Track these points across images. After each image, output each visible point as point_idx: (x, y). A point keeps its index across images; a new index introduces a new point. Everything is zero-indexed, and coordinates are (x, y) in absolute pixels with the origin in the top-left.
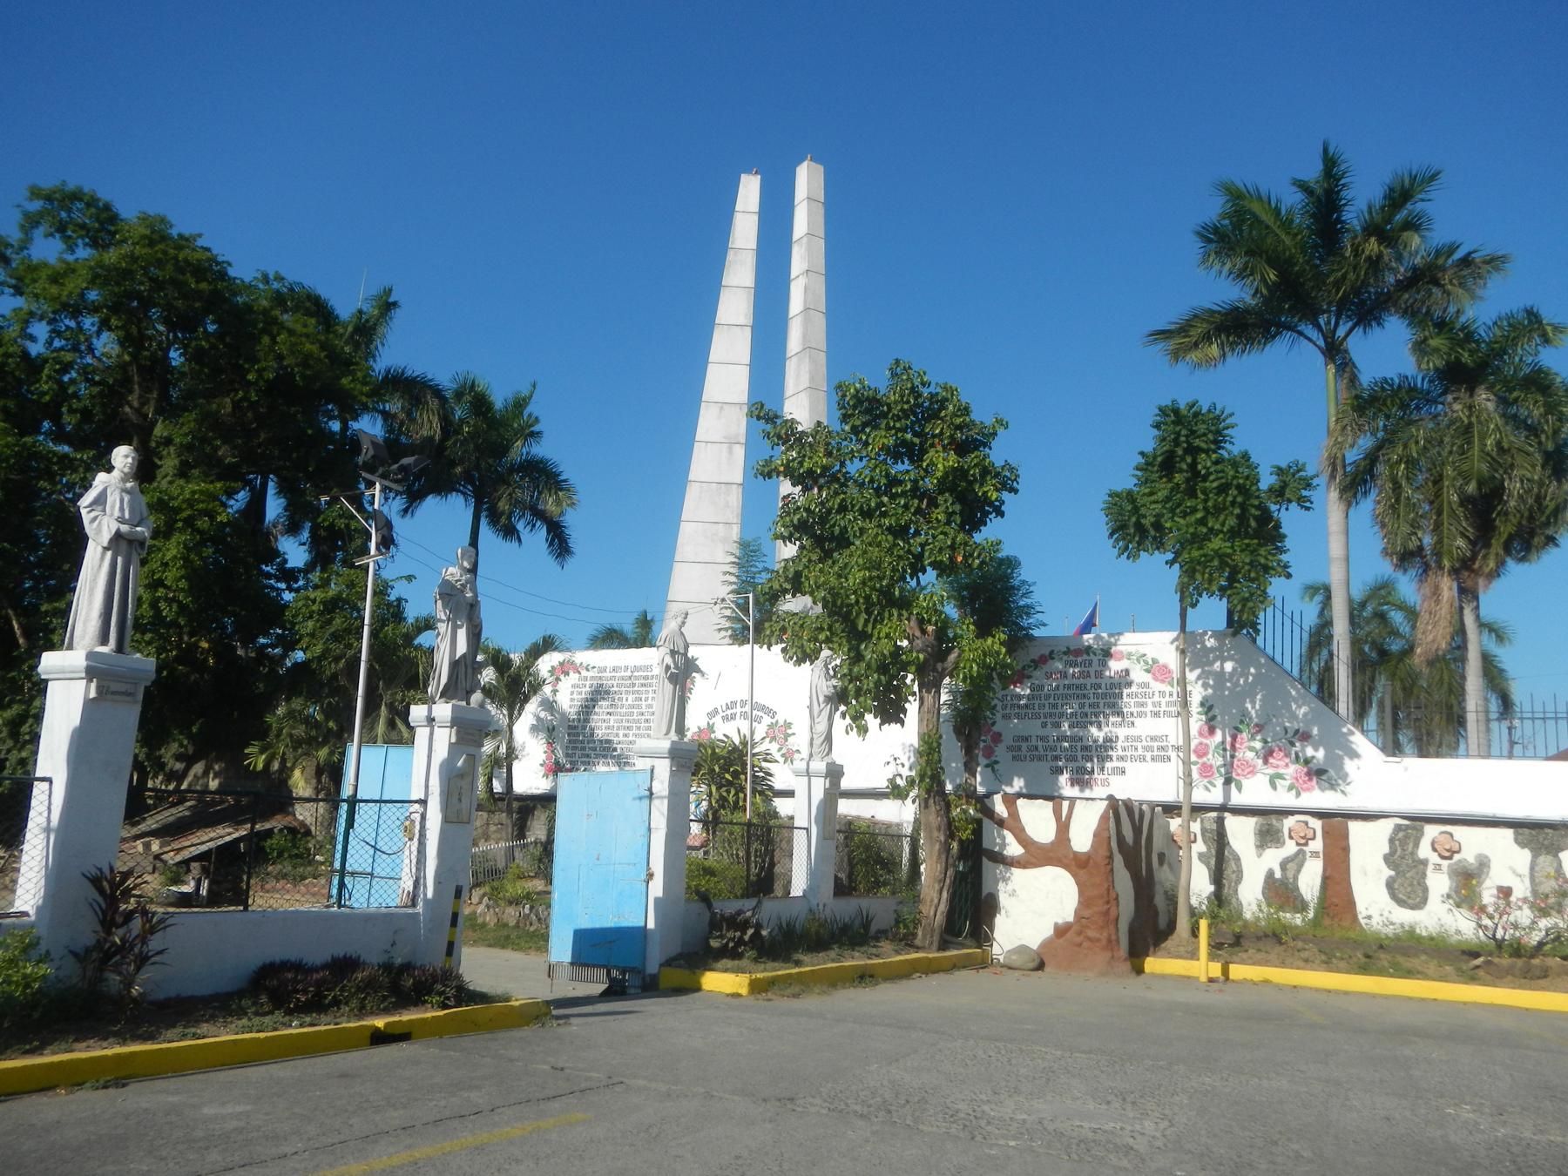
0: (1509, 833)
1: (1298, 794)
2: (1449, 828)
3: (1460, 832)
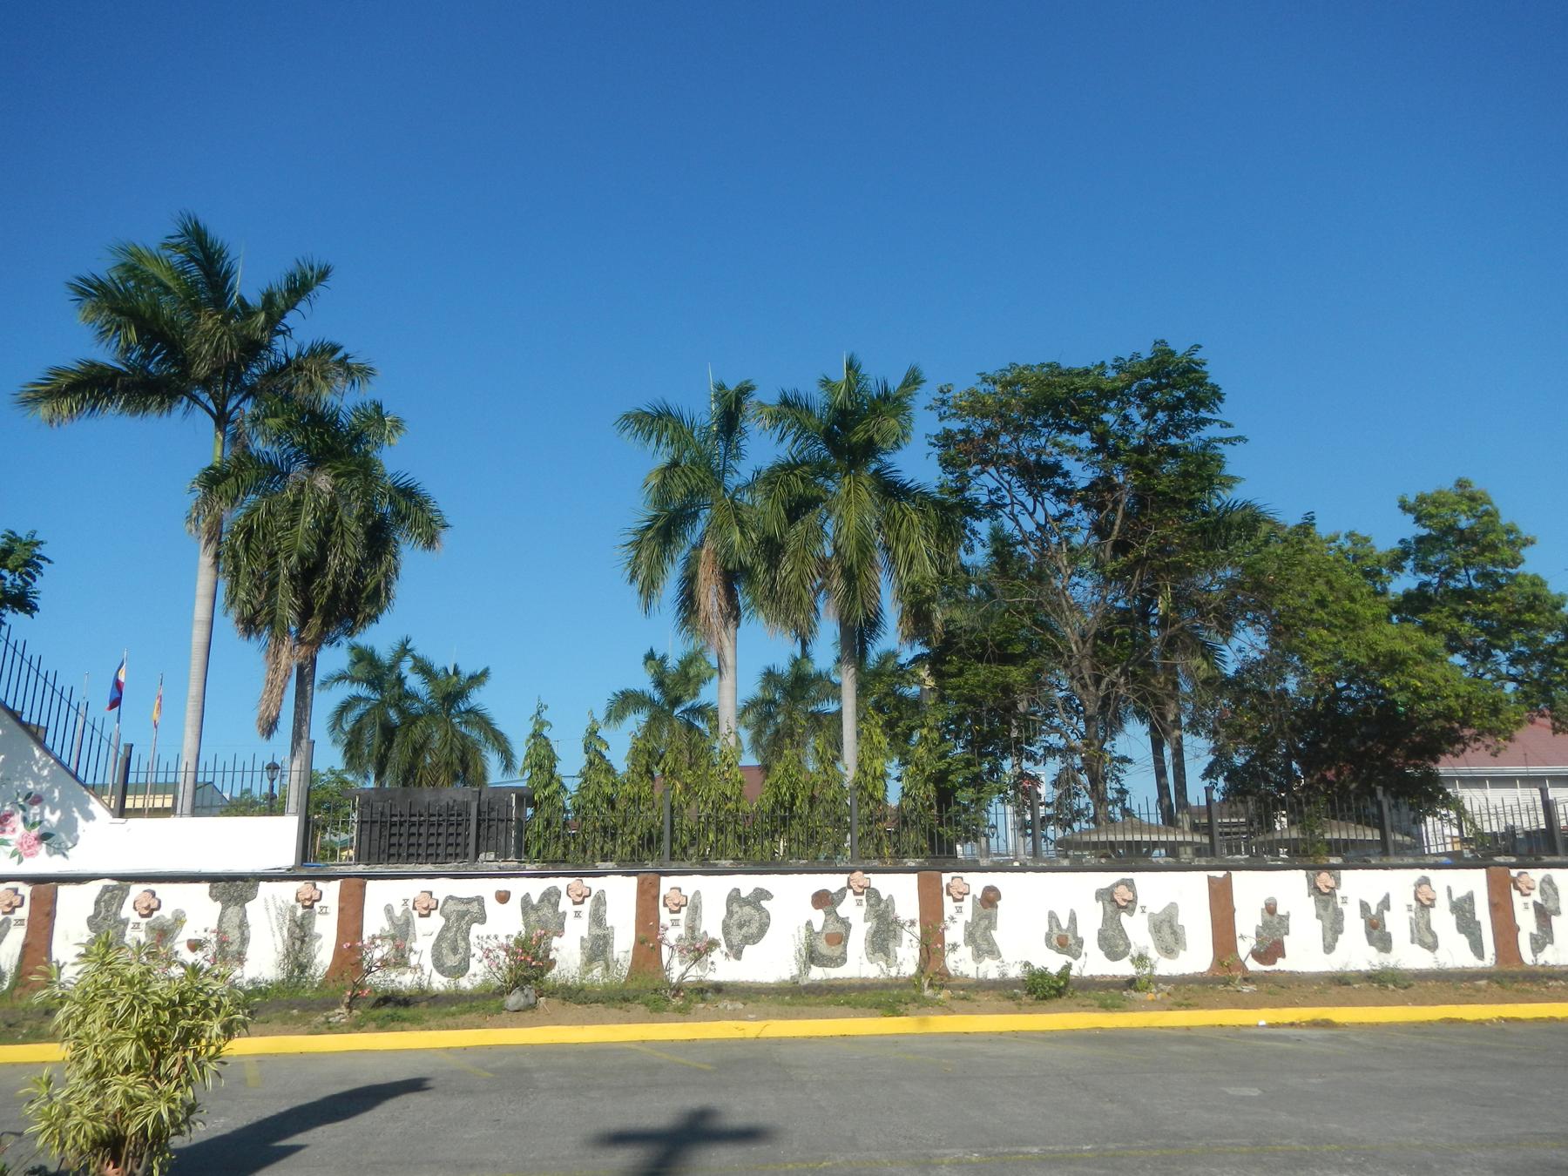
0: (205, 887)
1: (20, 861)
2: (153, 887)
3: (161, 889)
